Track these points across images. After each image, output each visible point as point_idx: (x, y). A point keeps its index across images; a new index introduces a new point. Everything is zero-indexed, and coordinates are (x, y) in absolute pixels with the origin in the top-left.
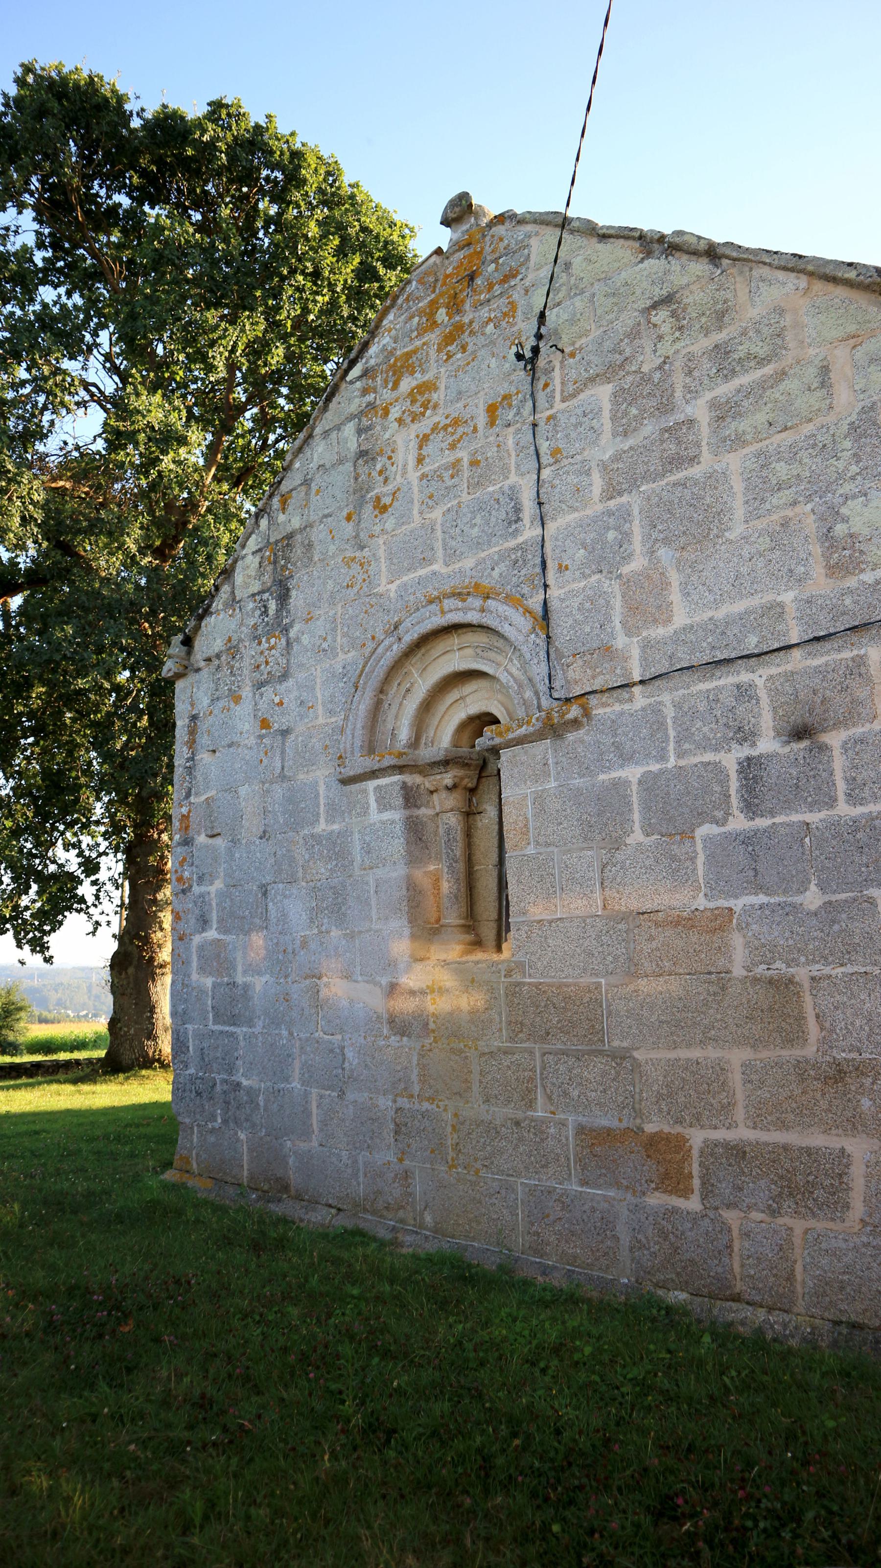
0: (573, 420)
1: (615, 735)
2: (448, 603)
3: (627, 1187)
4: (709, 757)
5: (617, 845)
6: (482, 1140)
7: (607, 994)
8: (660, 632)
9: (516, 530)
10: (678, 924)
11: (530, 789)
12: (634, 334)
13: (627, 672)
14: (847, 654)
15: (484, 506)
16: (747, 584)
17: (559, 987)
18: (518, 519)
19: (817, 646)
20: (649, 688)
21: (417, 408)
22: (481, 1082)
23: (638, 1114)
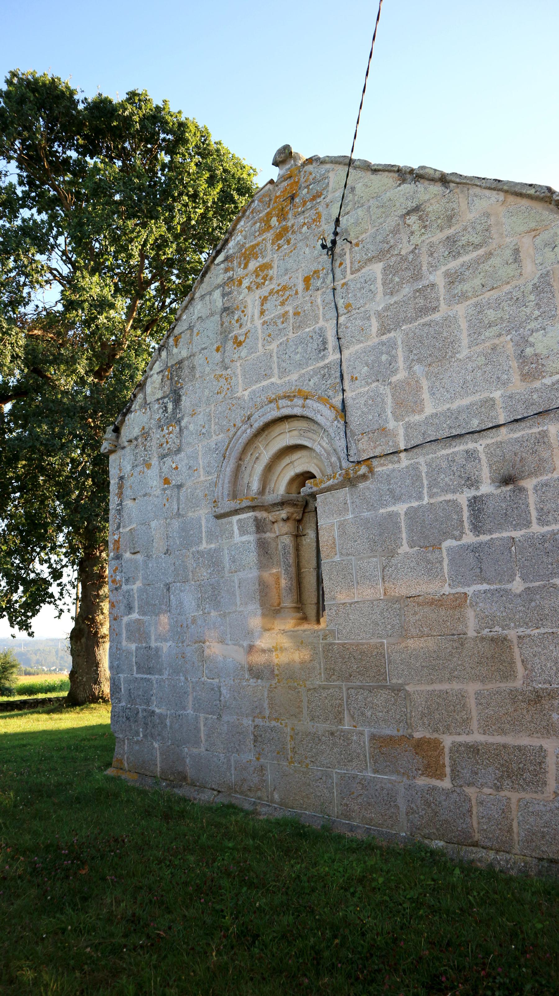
0: (358, 286)
1: (389, 484)
2: (282, 403)
3: (404, 773)
4: (449, 497)
5: (392, 554)
6: (310, 745)
7: (388, 649)
8: (416, 418)
9: (324, 355)
10: (432, 603)
11: (336, 520)
12: (395, 231)
13: (396, 444)
14: (535, 430)
15: (303, 341)
16: (471, 387)
17: (357, 645)
18: (325, 349)
19: (516, 425)
20: (410, 454)
21: (260, 280)
22: (308, 708)
23: (409, 726)
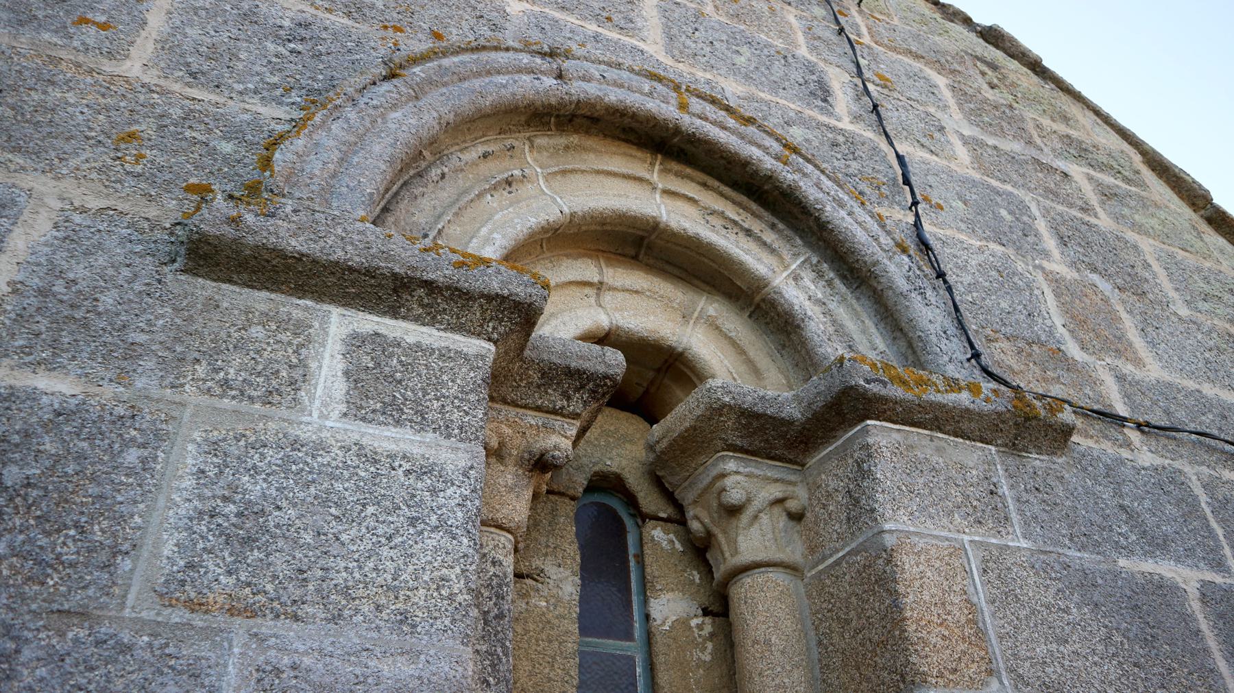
2: (696, 105)
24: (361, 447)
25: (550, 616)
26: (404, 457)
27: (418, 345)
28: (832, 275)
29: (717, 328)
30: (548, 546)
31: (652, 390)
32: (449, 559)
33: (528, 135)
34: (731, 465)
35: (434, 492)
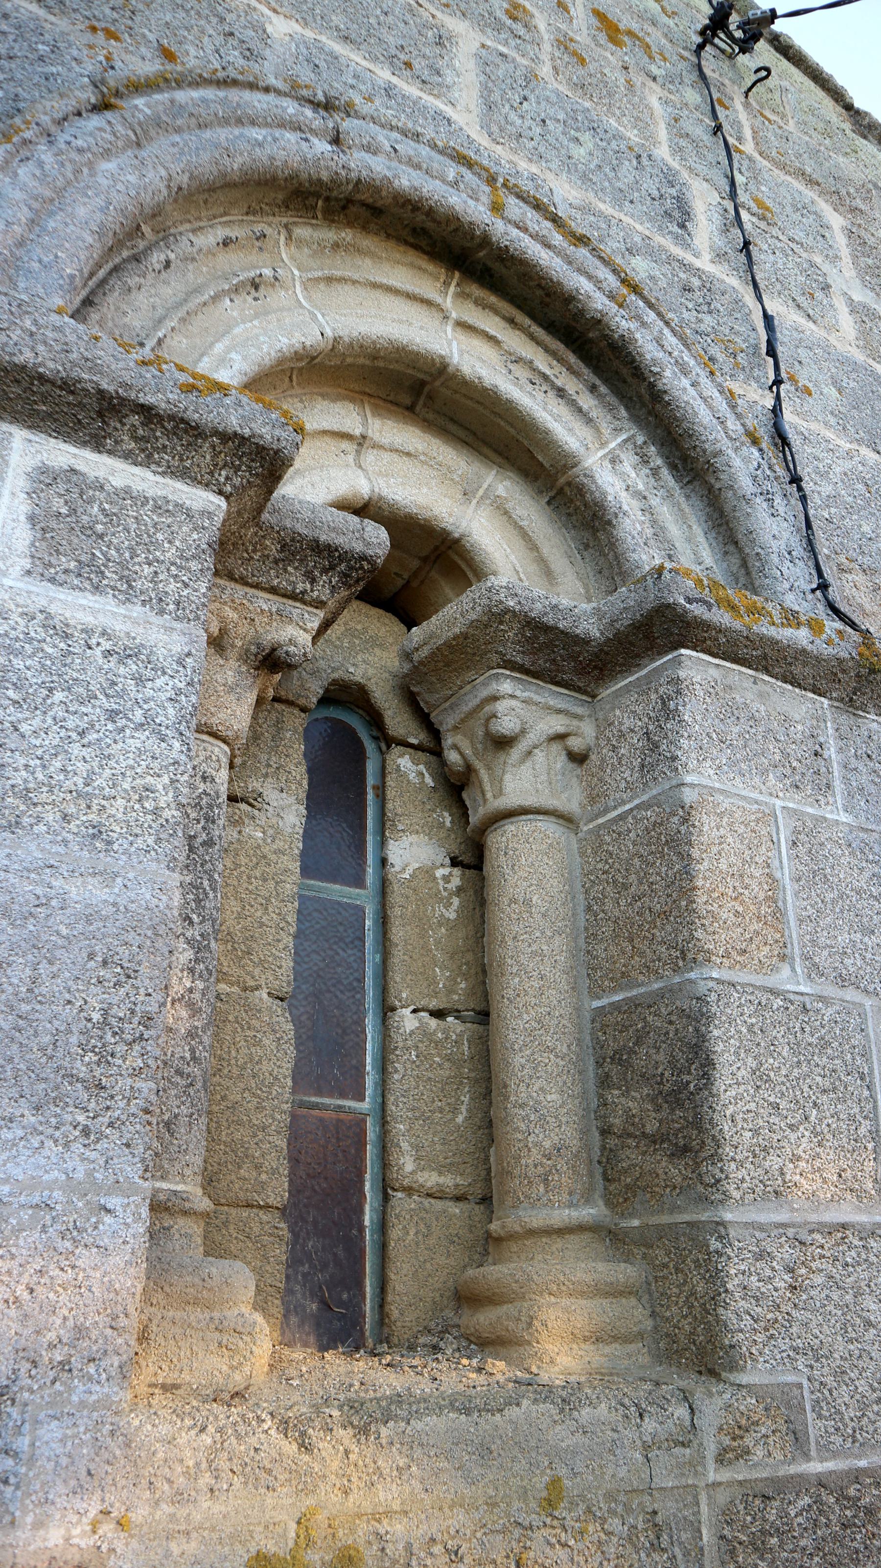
24: (49, 616)
25: (266, 850)
26: (104, 633)
27: (127, 490)
28: (659, 462)
29: (506, 513)
30: (269, 766)
31: (415, 584)
32: (156, 765)
33: (285, 220)
34: (506, 687)
35: (140, 680)
